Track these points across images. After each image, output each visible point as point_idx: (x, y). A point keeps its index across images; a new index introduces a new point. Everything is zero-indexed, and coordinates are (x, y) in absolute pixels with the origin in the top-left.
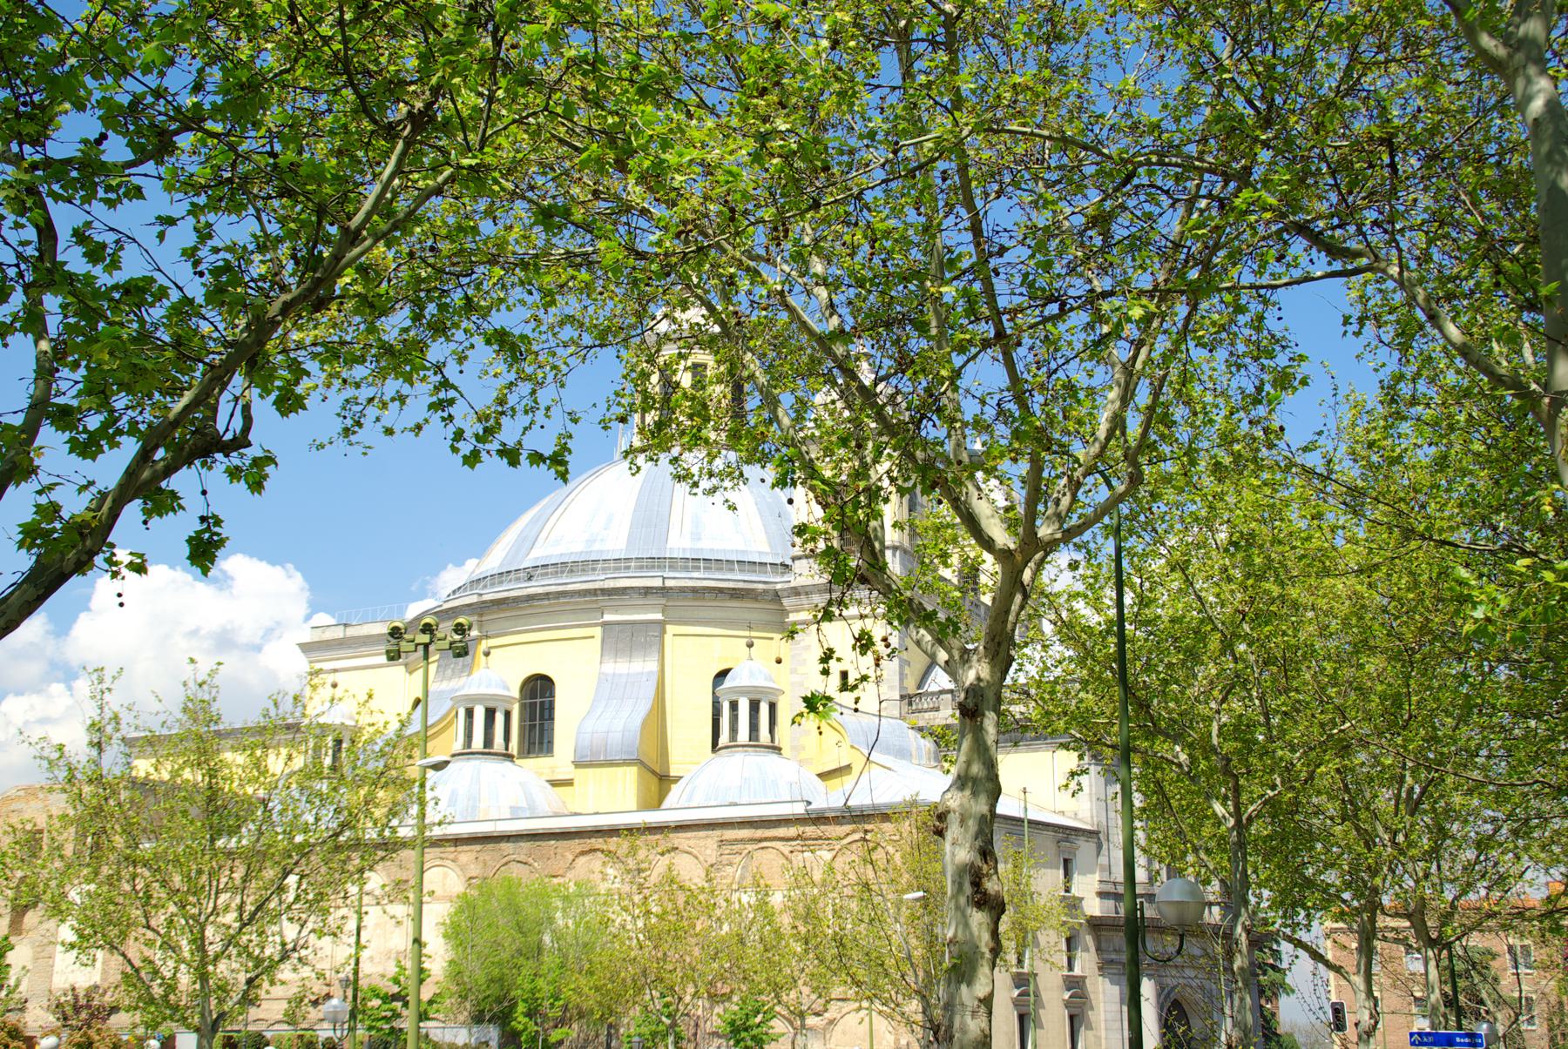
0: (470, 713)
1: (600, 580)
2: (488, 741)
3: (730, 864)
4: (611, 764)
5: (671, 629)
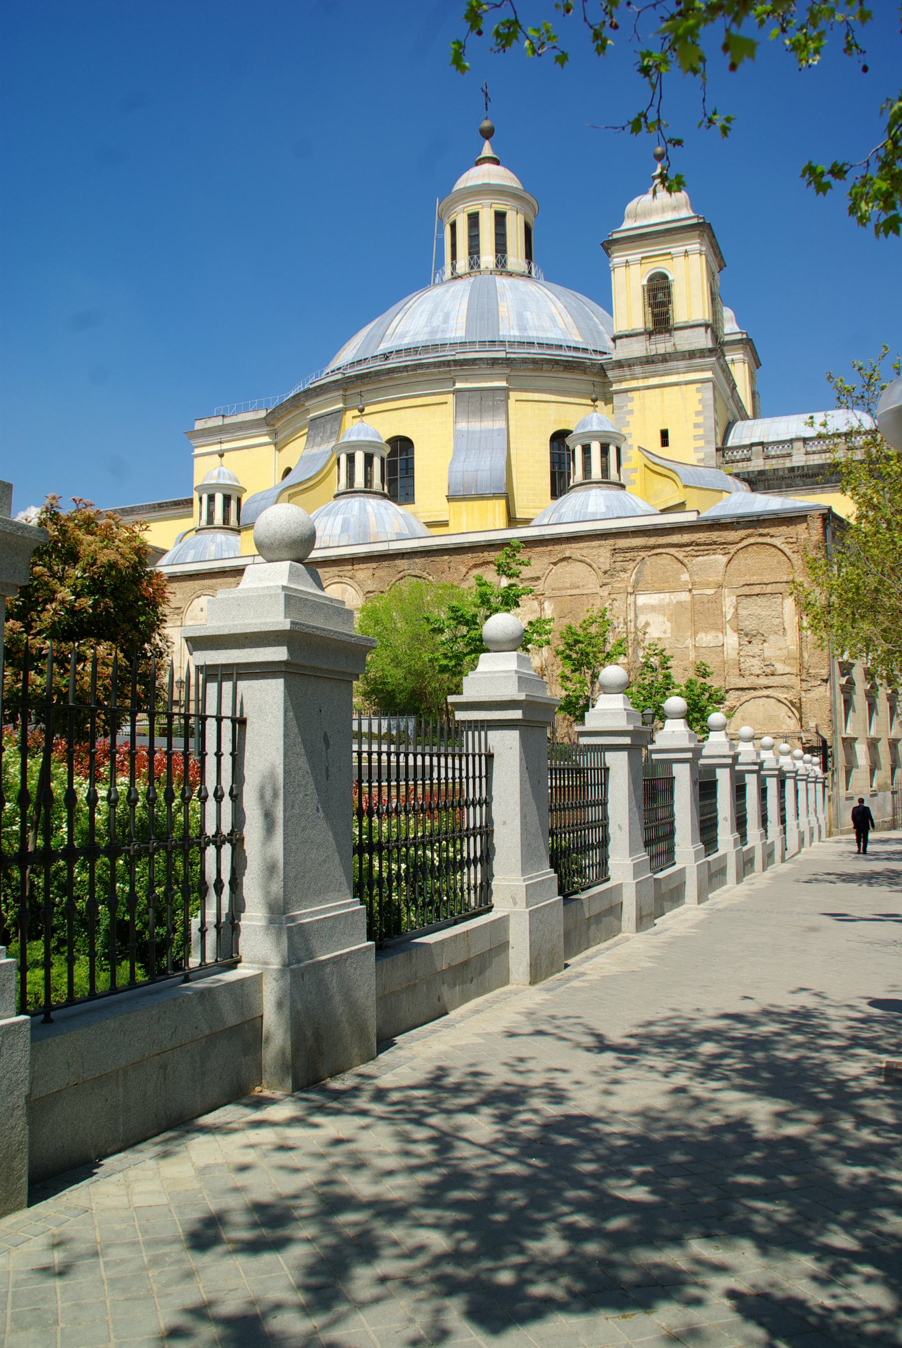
0: (351, 459)
1: (449, 355)
2: (368, 481)
4: (482, 497)
5: (513, 395)
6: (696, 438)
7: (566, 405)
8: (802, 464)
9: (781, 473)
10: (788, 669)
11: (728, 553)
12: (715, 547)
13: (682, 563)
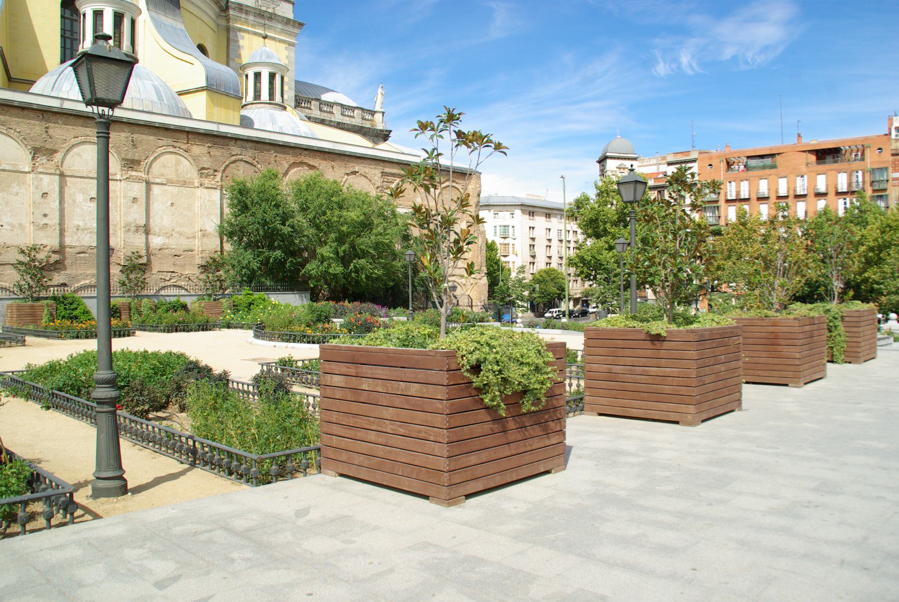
8: (340, 121)
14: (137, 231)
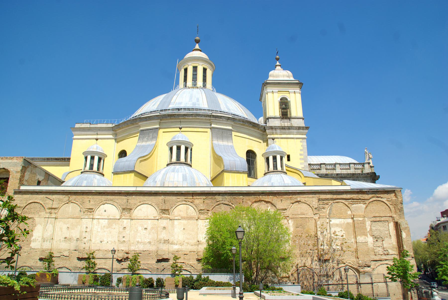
3: (324, 208)
6: (301, 159)
7: (251, 140)
8: (340, 173)
9: (333, 175)
10: (394, 252)
11: (366, 204)
12: (360, 201)
13: (348, 206)
14: (164, 243)
